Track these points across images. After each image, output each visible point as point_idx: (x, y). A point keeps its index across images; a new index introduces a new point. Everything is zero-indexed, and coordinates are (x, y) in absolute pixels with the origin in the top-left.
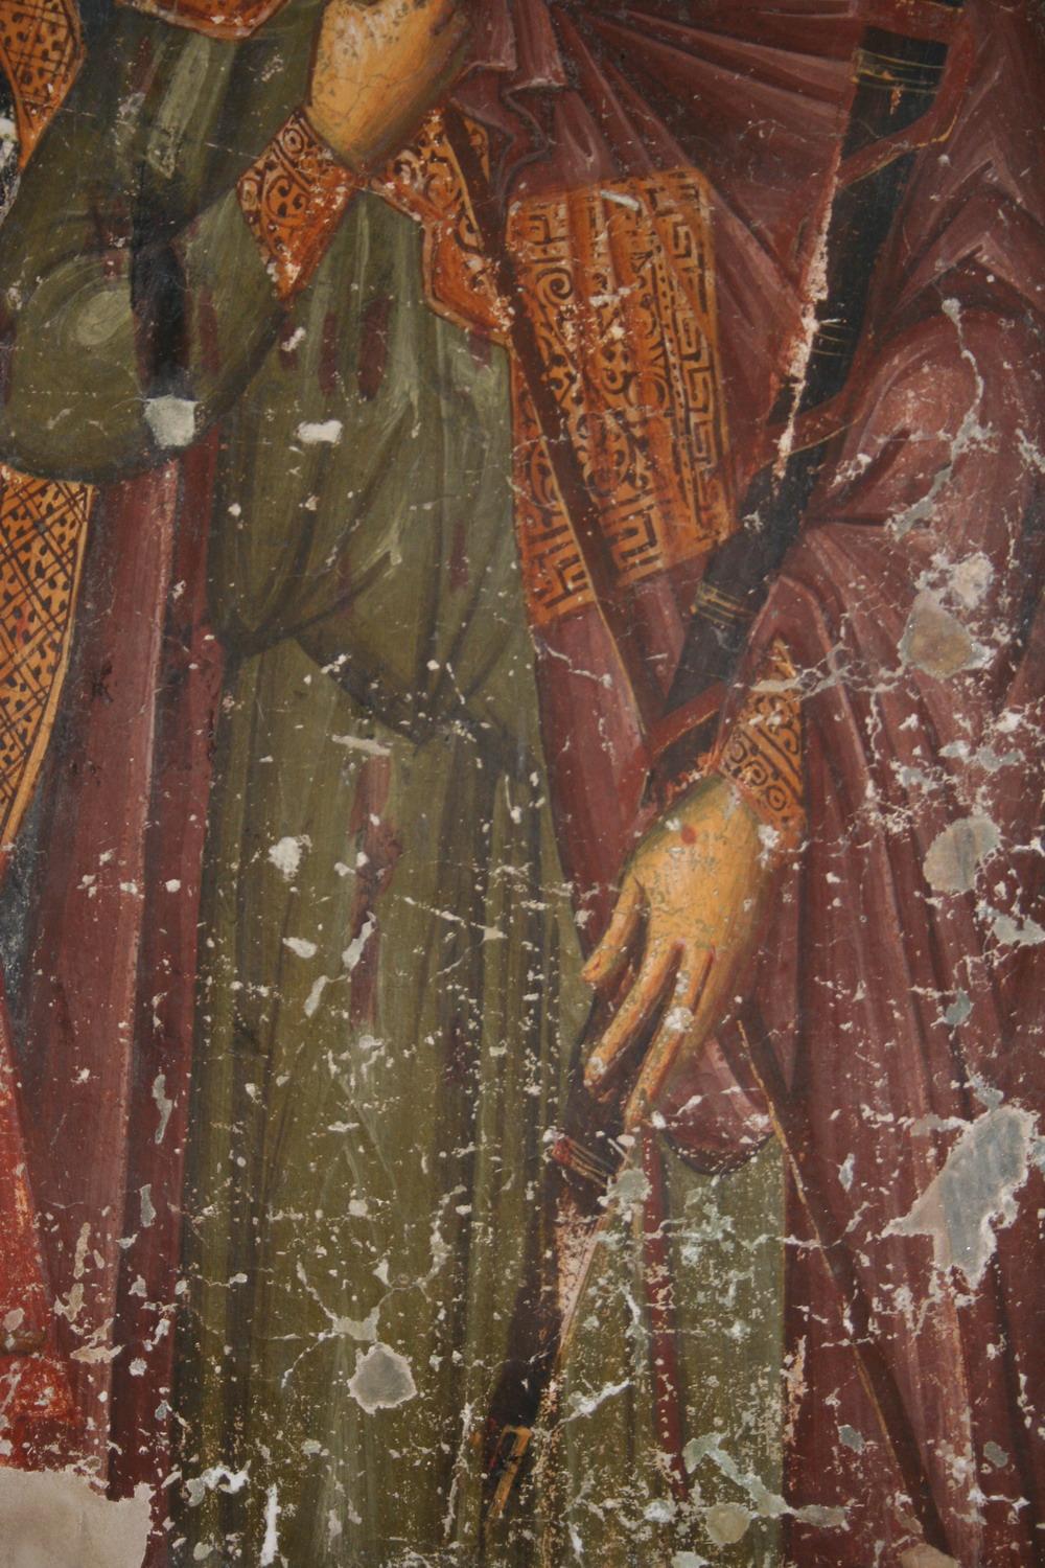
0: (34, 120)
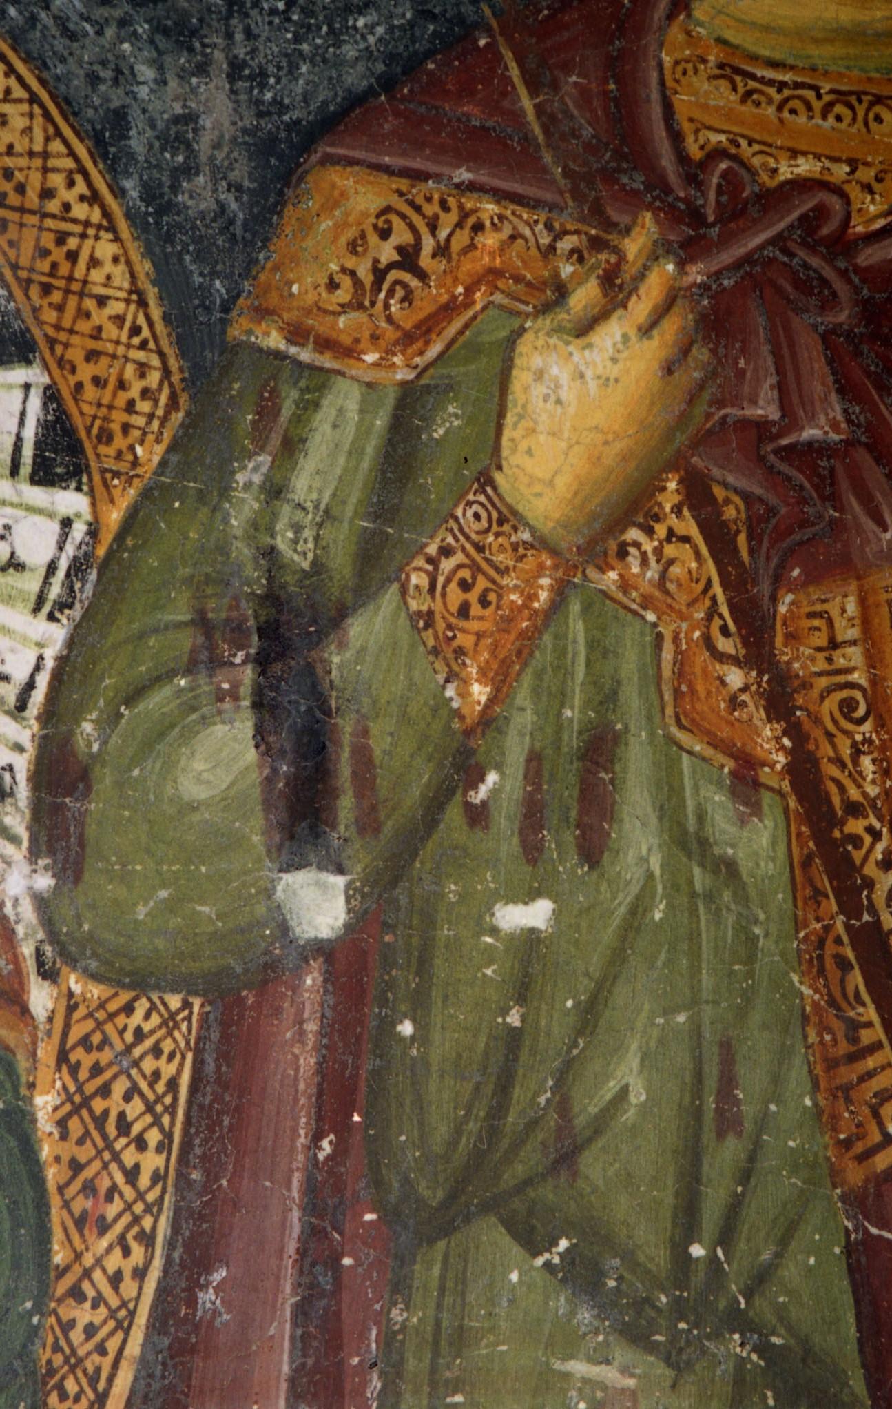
0: (116, 493)
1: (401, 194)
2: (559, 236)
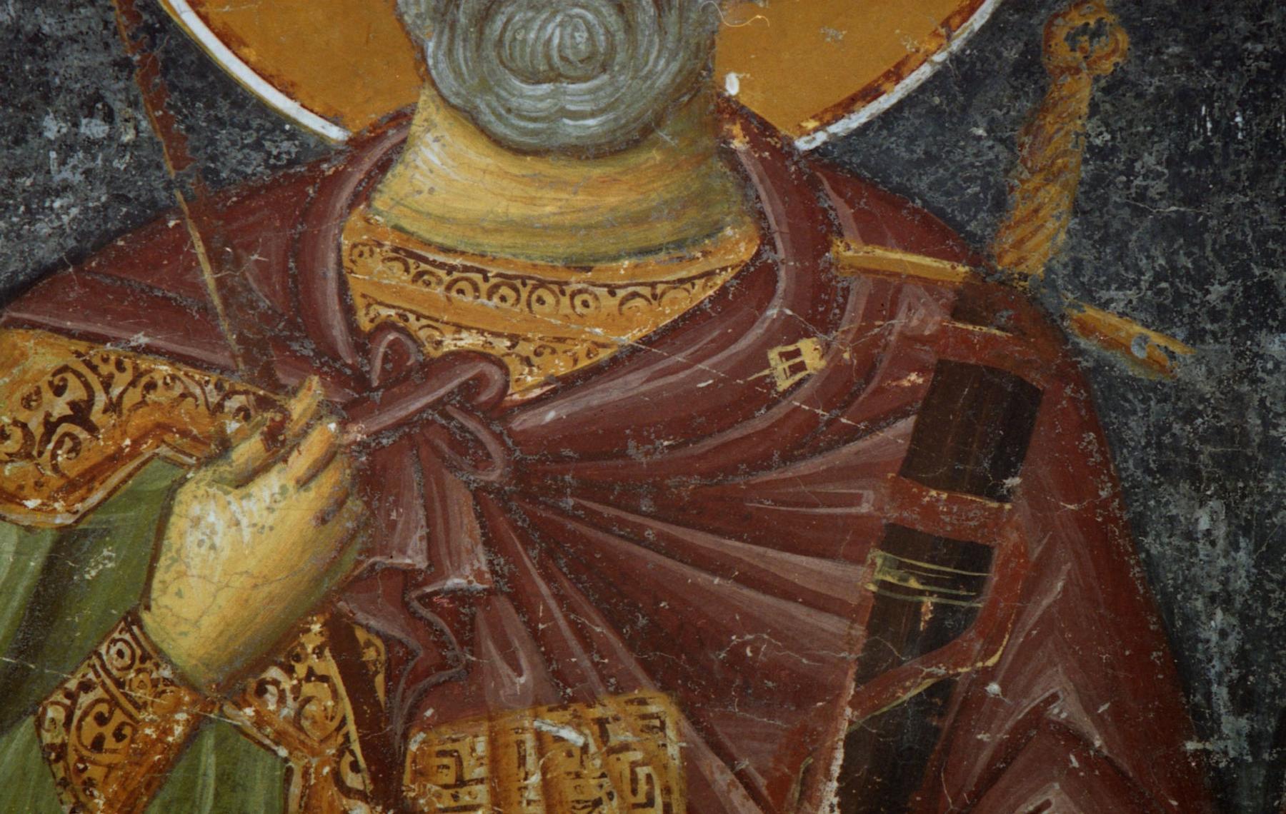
1: (79, 355)
2: (228, 396)
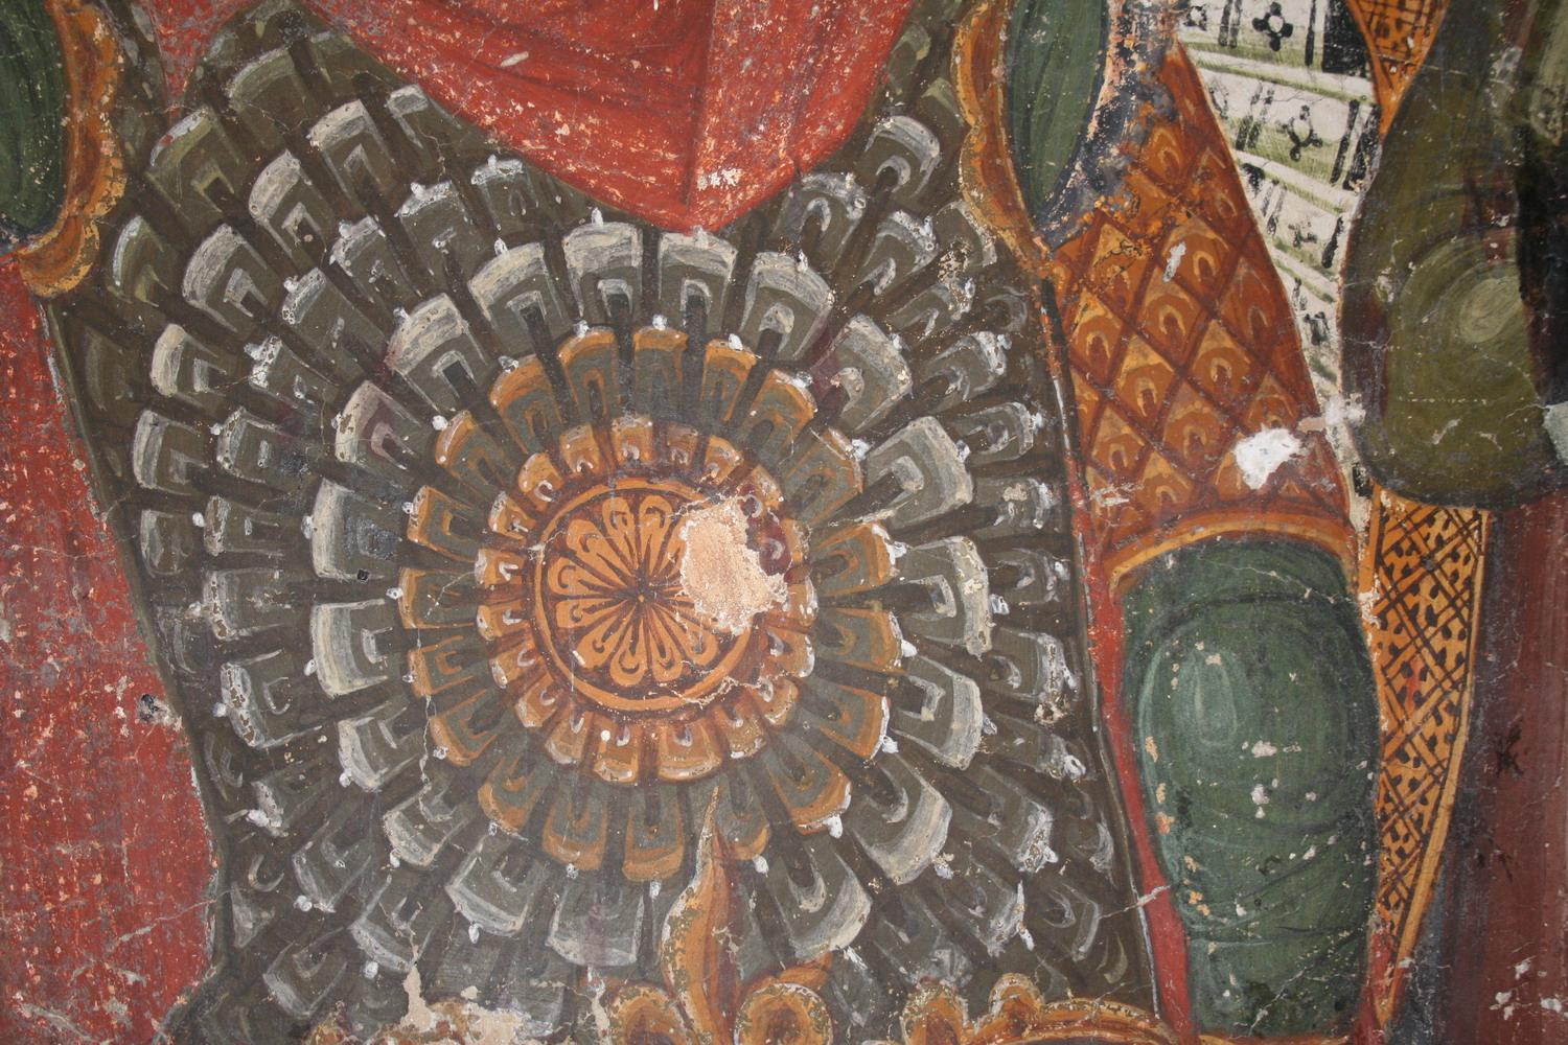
0: (1395, 79)
